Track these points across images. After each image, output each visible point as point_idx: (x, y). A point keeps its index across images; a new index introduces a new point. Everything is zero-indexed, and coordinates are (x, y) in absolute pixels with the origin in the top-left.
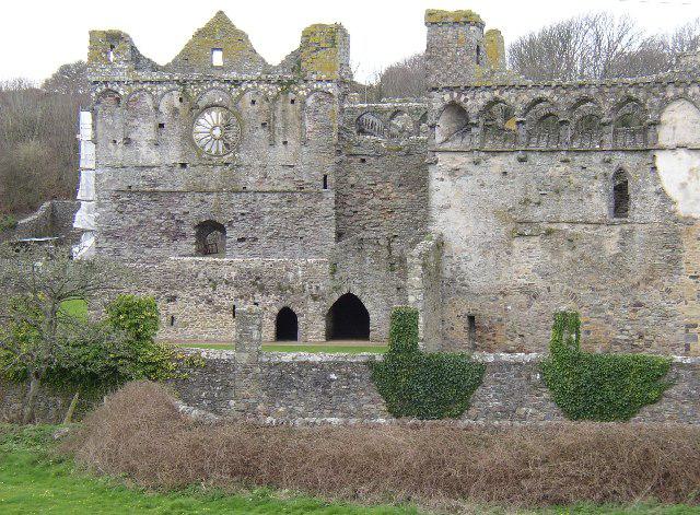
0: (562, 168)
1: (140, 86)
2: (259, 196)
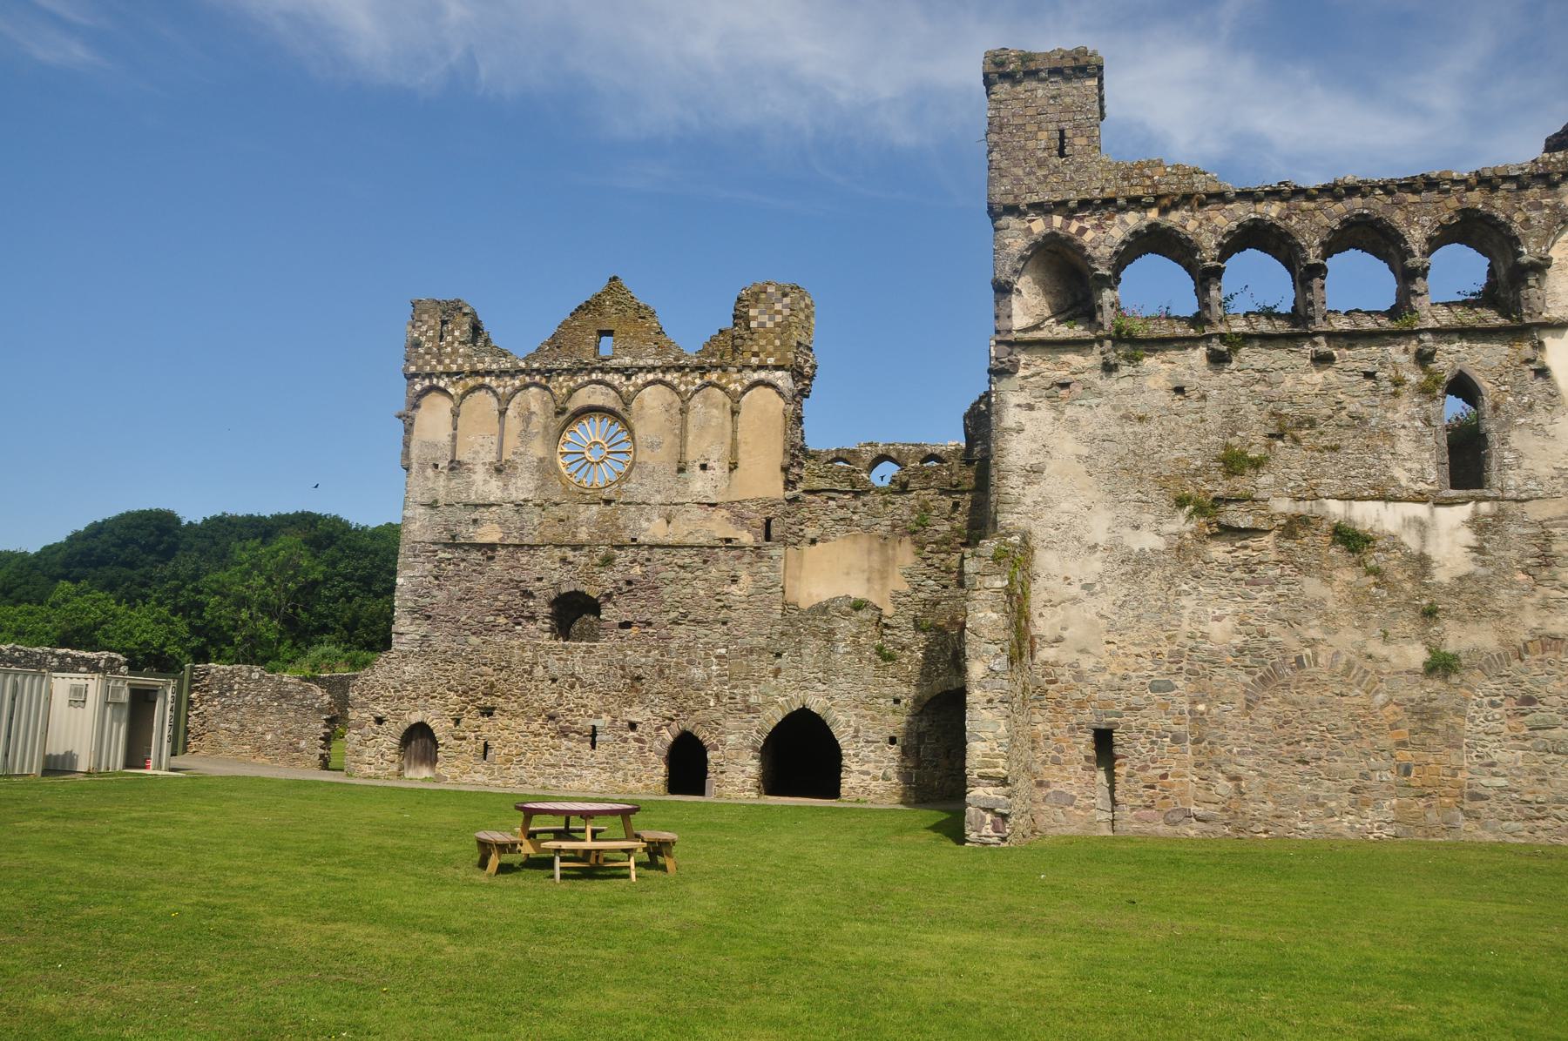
0: (1317, 377)
1: (480, 380)
2: (658, 553)
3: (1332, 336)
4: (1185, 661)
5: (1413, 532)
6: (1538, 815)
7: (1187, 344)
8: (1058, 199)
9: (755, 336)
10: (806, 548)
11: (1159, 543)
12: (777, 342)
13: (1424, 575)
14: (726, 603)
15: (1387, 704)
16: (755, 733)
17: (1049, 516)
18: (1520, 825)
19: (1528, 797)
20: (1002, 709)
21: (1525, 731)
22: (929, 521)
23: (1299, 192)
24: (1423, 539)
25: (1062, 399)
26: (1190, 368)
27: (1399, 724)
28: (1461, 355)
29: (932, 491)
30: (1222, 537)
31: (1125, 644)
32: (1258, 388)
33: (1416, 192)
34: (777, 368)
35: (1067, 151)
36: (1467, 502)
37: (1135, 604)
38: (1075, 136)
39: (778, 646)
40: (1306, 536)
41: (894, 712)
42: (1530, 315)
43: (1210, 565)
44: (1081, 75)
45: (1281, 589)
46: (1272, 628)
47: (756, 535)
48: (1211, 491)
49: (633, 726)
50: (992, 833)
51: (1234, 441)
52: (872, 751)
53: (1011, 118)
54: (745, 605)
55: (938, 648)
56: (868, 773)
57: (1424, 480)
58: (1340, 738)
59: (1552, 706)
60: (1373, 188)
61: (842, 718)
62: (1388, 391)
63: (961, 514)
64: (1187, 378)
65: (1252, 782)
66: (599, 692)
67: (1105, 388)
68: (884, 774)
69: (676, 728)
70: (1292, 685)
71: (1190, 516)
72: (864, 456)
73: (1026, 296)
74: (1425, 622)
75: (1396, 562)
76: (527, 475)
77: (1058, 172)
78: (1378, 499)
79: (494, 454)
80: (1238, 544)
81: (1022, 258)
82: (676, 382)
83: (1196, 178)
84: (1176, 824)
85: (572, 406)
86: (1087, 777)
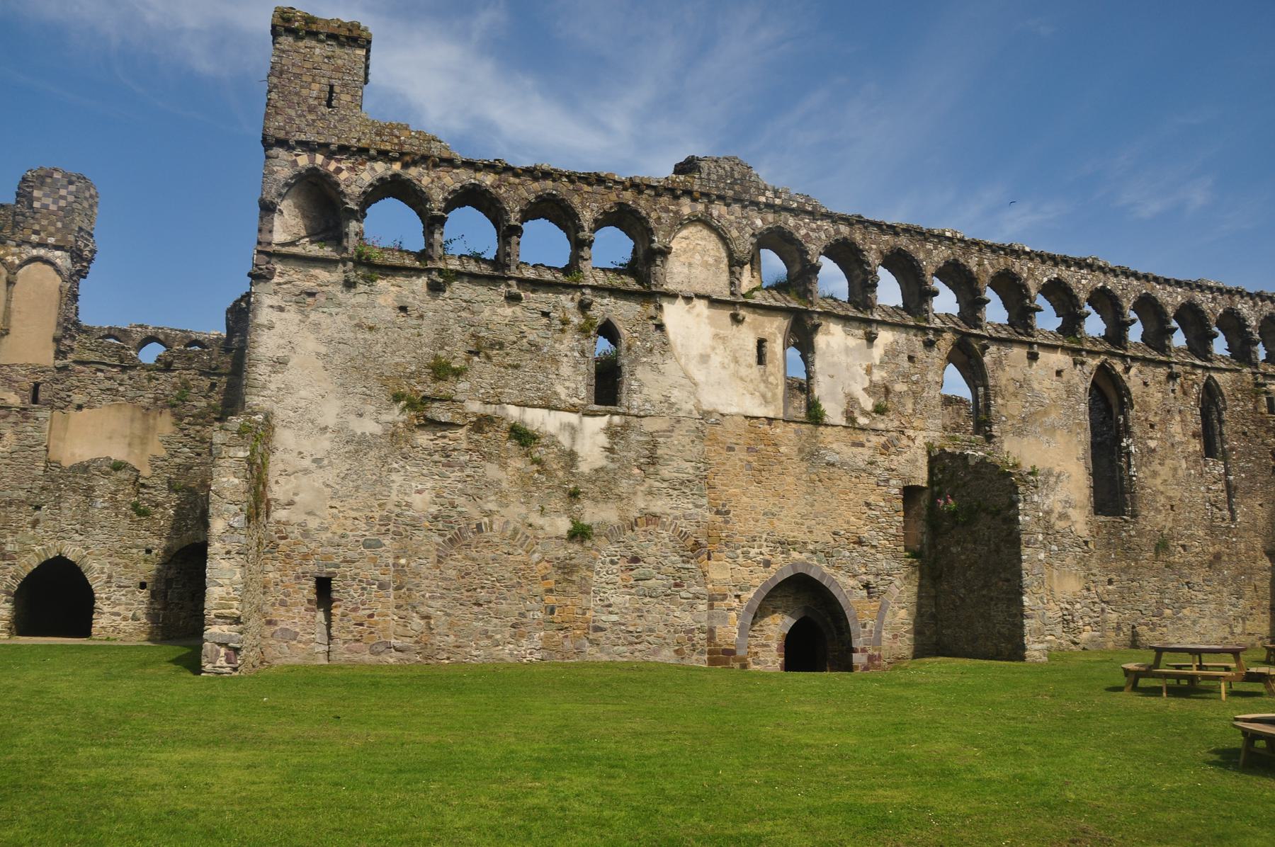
0: (508, 311)
3: (522, 282)
4: (392, 524)
5: (567, 434)
6: (636, 641)
7: (412, 273)
8: (322, 141)
9: (38, 216)
10: (72, 413)
11: (377, 429)
12: (59, 225)
13: (572, 467)
15: (540, 561)
16: (9, 579)
17: (290, 401)
18: (624, 648)
19: (631, 629)
20: (238, 559)
21: (632, 582)
22: (188, 398)
23: (508, 169)
24: (573, 439)
25: (308, 305)
26: (413, 292)
27: (548, 576)
28: (609, 307)
29: (193, 372)
30: (427, 428)
31: (345, 509)
32: (463, 314)
33: (590, 184)
34: (57, 248)
35: (334, 103)
36: (605, 415)
37: (355, 477)
38: (342, 92)
39: (38, 499)
40: (490, 431)
41: (146, 561)
42: (656, 285)
43: (416, 449)
44: (353, 44)
45: (469, 471)
46: (460, 500)
47: (23, 397)
48: (421, 391)
50: (225, 664)
51: (442, 353)
52: (123, 595)
53: (290, 67)
54: (7, 461)
55: (188, 507)
56: (118, 614)
57: (577, 396)
58: (506, 586)
59: (650, 564)
60: (561, 175)
61: (96, 565)
62: (558, 327)
63: (217, 393)
64: (410, 300)
65: (439, 620)
67: (344, 301)
68: (134, 615)
70: (473, 545)
71: (403, 409)
72: (134, 336)
73: (286, 217)
74: (571, 501)
75: (553, 456)
77: (325, 119)
78: (544, 408)
80: (439, 434)
81: (286, 184)
83: (433, 145)
84: (379, 653)
86: (308, 617)
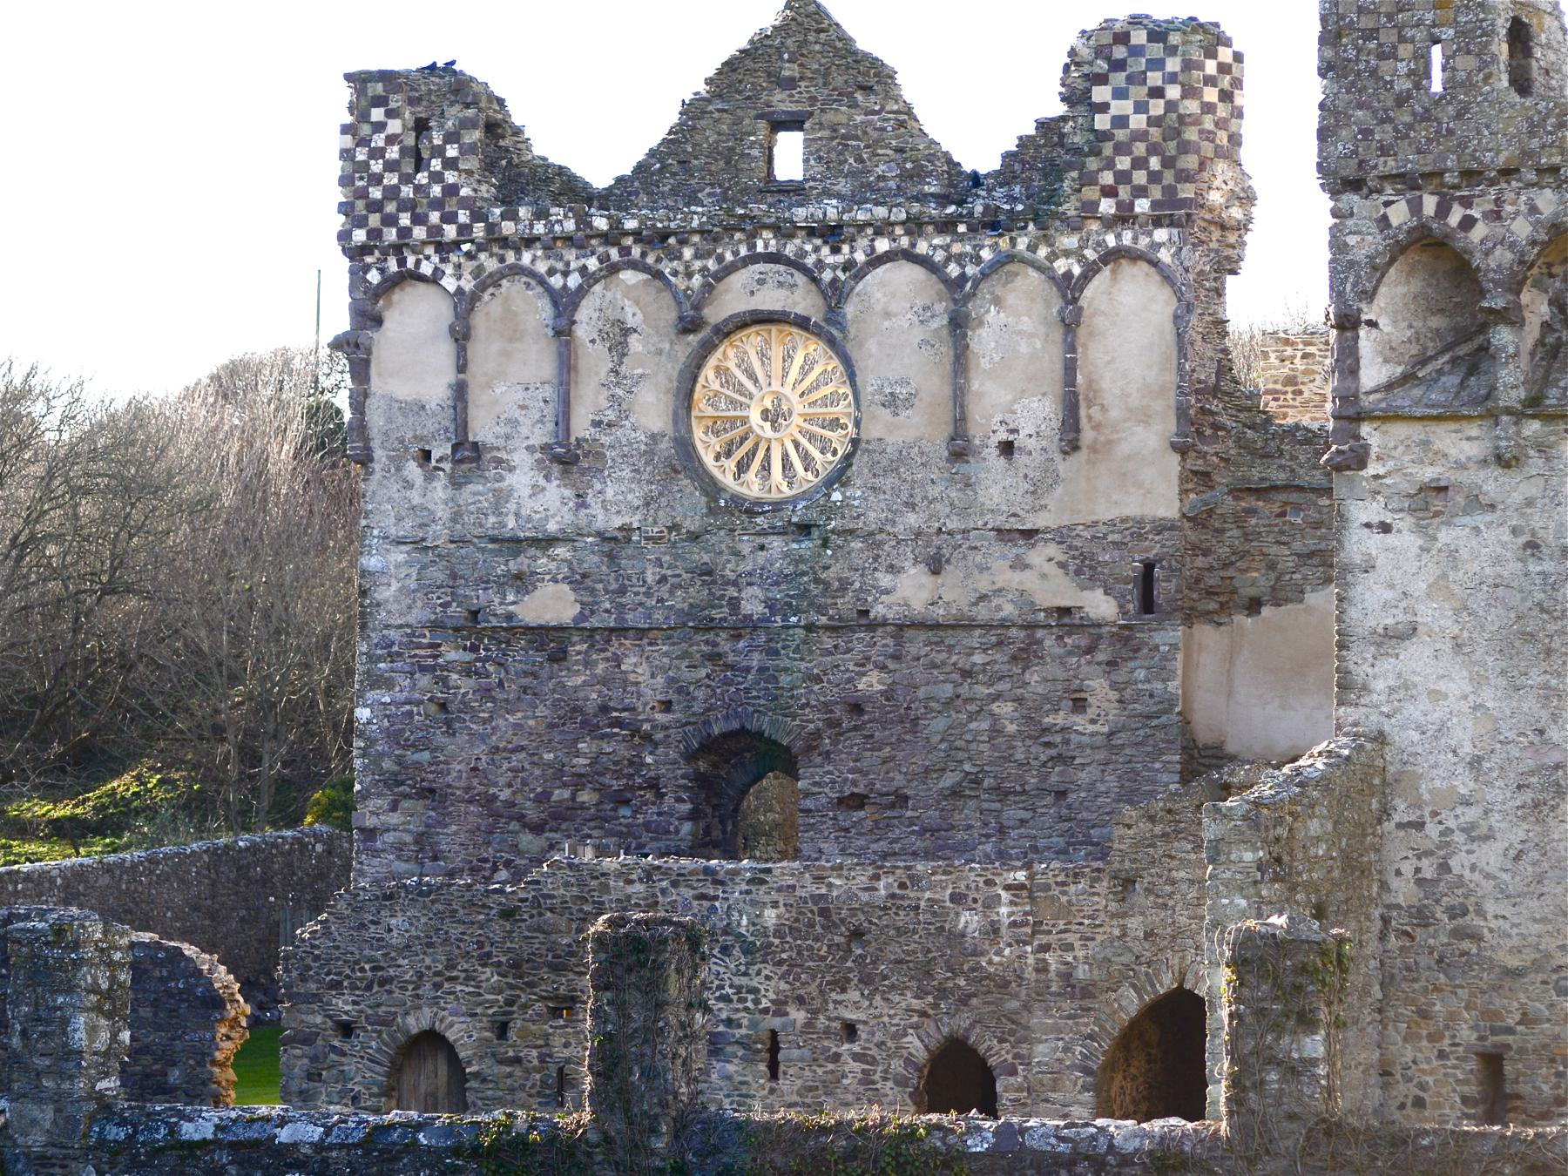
9: (1108, 149)
10: (1243, 621)
12: (1155, 163)
14: (1062, 749)
34: (1158, 222)
49: (850, 1031)
66: (780, 963)
69: (937, 1034)
76: (627, 473)
77: (1429, 119)
79: (550, 426)
82: (939, 256)
85: (716, 313)
